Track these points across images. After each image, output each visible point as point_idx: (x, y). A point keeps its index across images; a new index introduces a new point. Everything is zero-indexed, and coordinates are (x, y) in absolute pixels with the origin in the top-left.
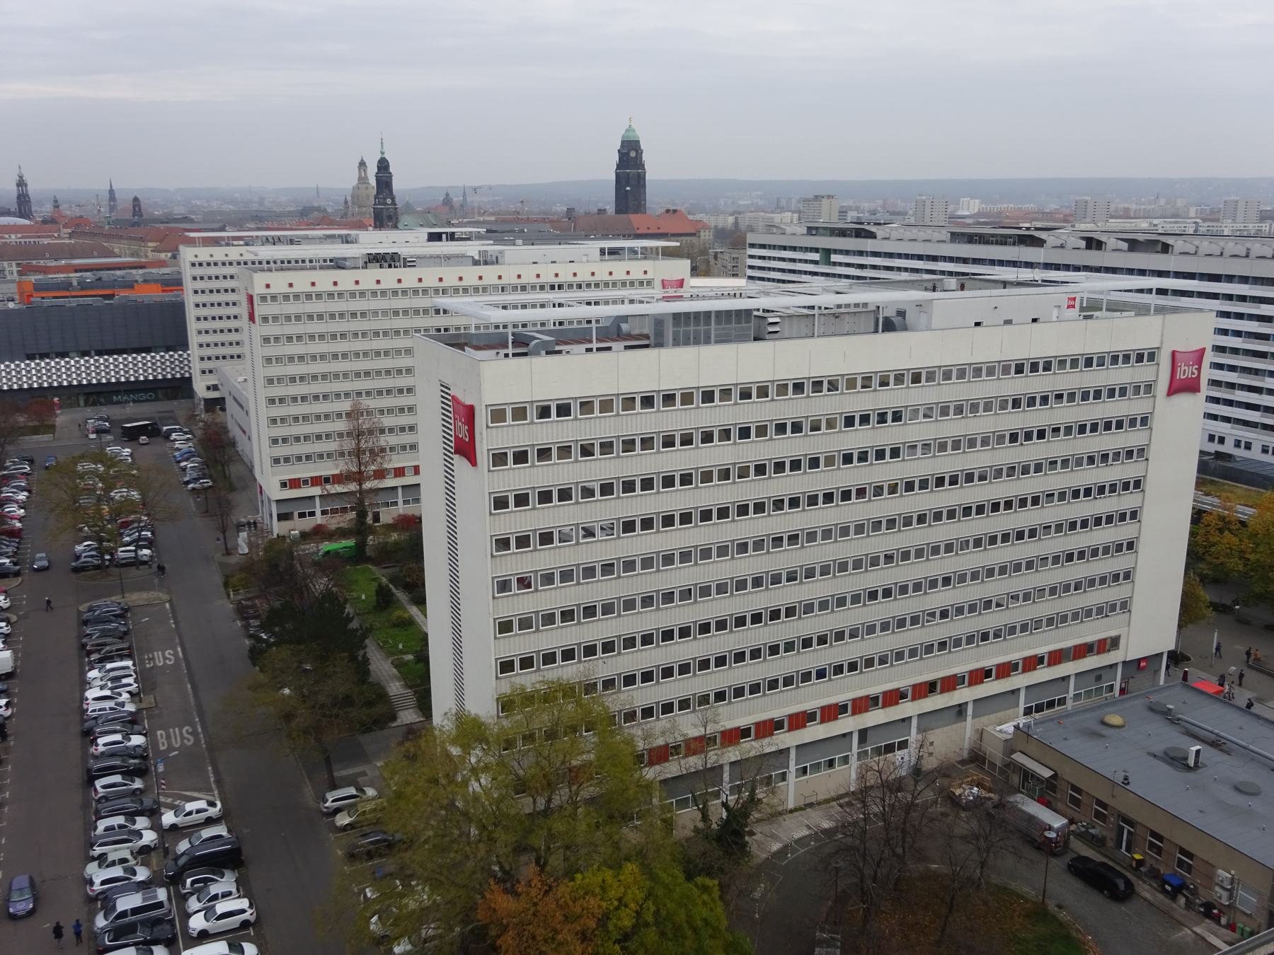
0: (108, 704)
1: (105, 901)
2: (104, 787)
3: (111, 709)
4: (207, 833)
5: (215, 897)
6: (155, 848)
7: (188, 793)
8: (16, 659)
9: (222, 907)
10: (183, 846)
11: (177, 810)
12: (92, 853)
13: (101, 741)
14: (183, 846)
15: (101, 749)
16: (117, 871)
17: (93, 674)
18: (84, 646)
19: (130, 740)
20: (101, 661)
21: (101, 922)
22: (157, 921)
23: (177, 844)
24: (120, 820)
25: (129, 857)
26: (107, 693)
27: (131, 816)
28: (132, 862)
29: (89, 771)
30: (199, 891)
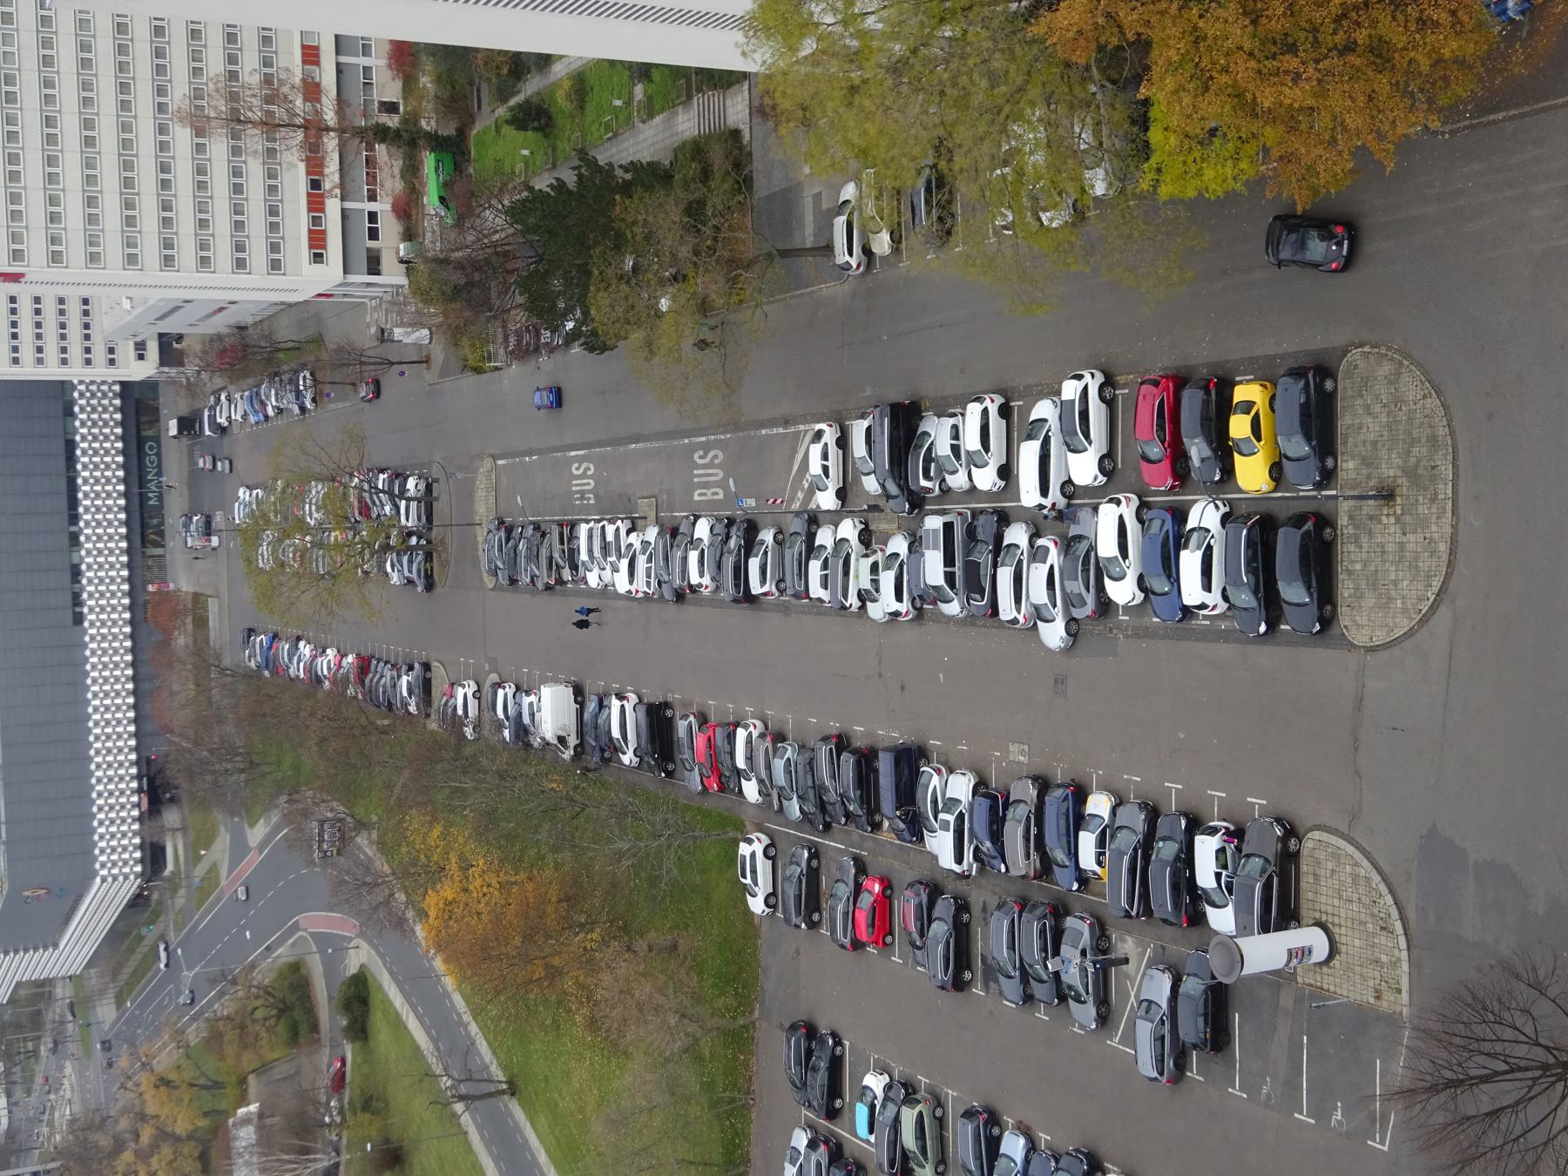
0: (641, 563)
1: (925, 601)
2: (763, 581)
3: (649, 560)
4: (859, 448)
5: (956, 450)
6: (866, 524)
7: (796, 467)
8: (555, 681)
9: (971, 441)
10: (871, 484)
11: (817, 487)
12: (854, 609)
13: (694, 579)
14: (871, 484)
15: (706, 580)
16: (887, 579)
17: (593, 579)
18: (548, 588)
19: (700, 540)
20: (574, 567)
21: (953, 608)
22: (971, 532)
23: (868, 493)
24: (815, 567)
25: (871, 560)
26: (624, 563)
27: (811, 549)
28: (879, 557)
29: (735, 601)
30: (940, 470)
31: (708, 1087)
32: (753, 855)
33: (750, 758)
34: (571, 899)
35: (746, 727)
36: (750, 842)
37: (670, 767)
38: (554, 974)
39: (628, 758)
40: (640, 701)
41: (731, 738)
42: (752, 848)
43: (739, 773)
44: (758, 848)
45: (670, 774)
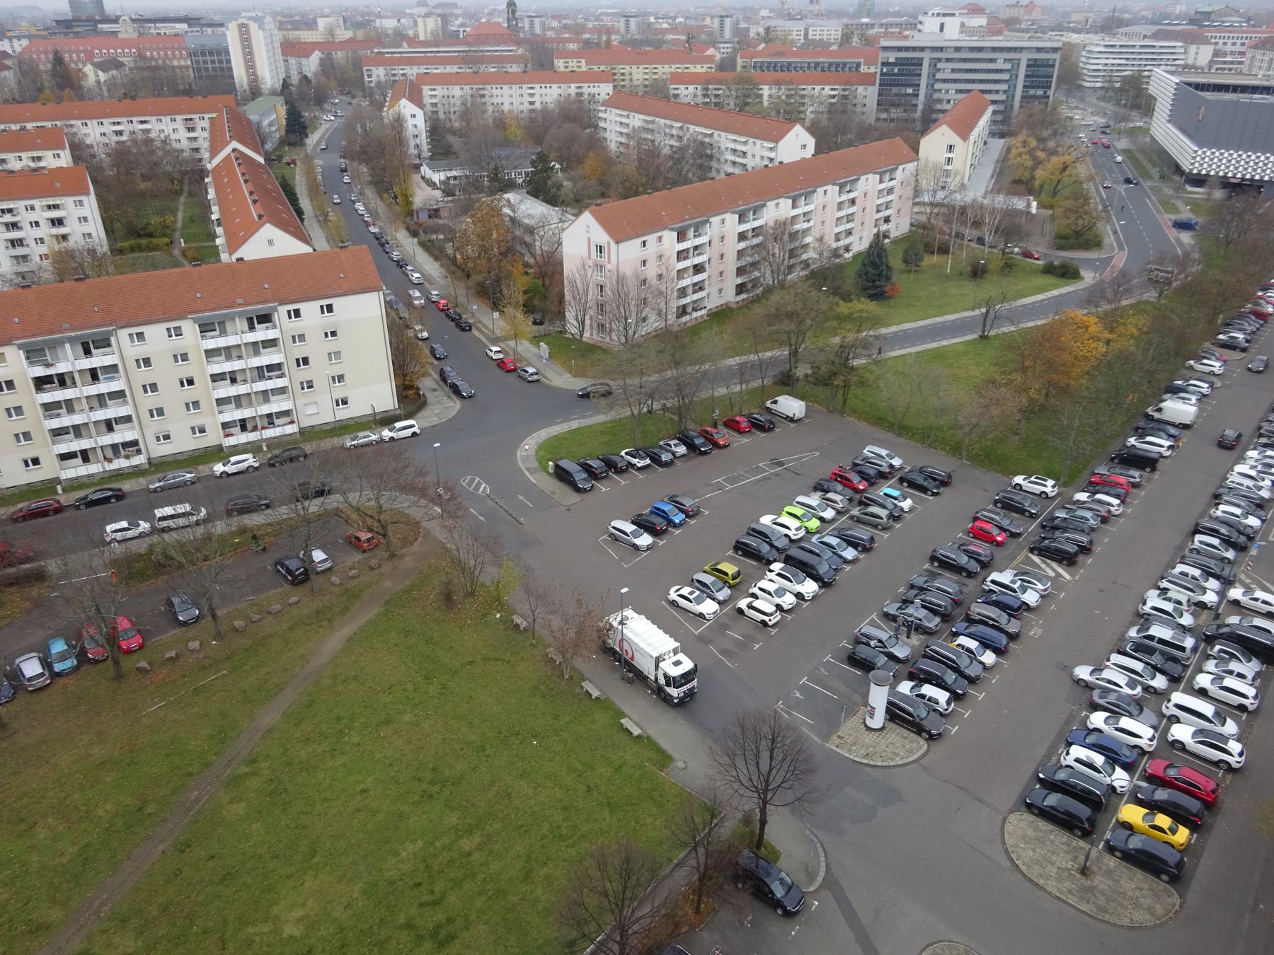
0: (1250, 483)
1: (1145, 620)
2: (1201, 542)
3: (1248, 487)
4: (1258, 622)
5: (1231, 672)
6: (1210, 609)
7: (1268, 585)
8: (1199, 416)
9: (1230, 682)
10: (1234, 620)
11: (1248, 590)
12: (1160, 584)
13: (1222, 507)
14: (1234, 620)
15: (1219, 513)
16: (1169, 607)
17: (1253, 454)
18: (1260, 428)
19: (1247, 518)
20: (1266, 446)
21: (1133, 633)
22: (1175, 660)
23: (1228, 616)
24: (1196, 572)
25: (1184, 602)
26: (1253, 473)
27: (1208, 574)
28: (1185, 607)
29: (1197, 525)
30: (1222, 659)
31: (939, 429)
32: (1045, 486)
33: (1100, 501)
34: (1065, 390)
35: (1119, 505)
36: (1053, 487)
37: (1116, 461)
38: (1024, 370)
39: (1132, 441)
40: (1162, 456)
41: (1117, 496)
42: (1049, 487)
43: (1095, 493)
44: (1048, 490)
45: (1112, 459)
